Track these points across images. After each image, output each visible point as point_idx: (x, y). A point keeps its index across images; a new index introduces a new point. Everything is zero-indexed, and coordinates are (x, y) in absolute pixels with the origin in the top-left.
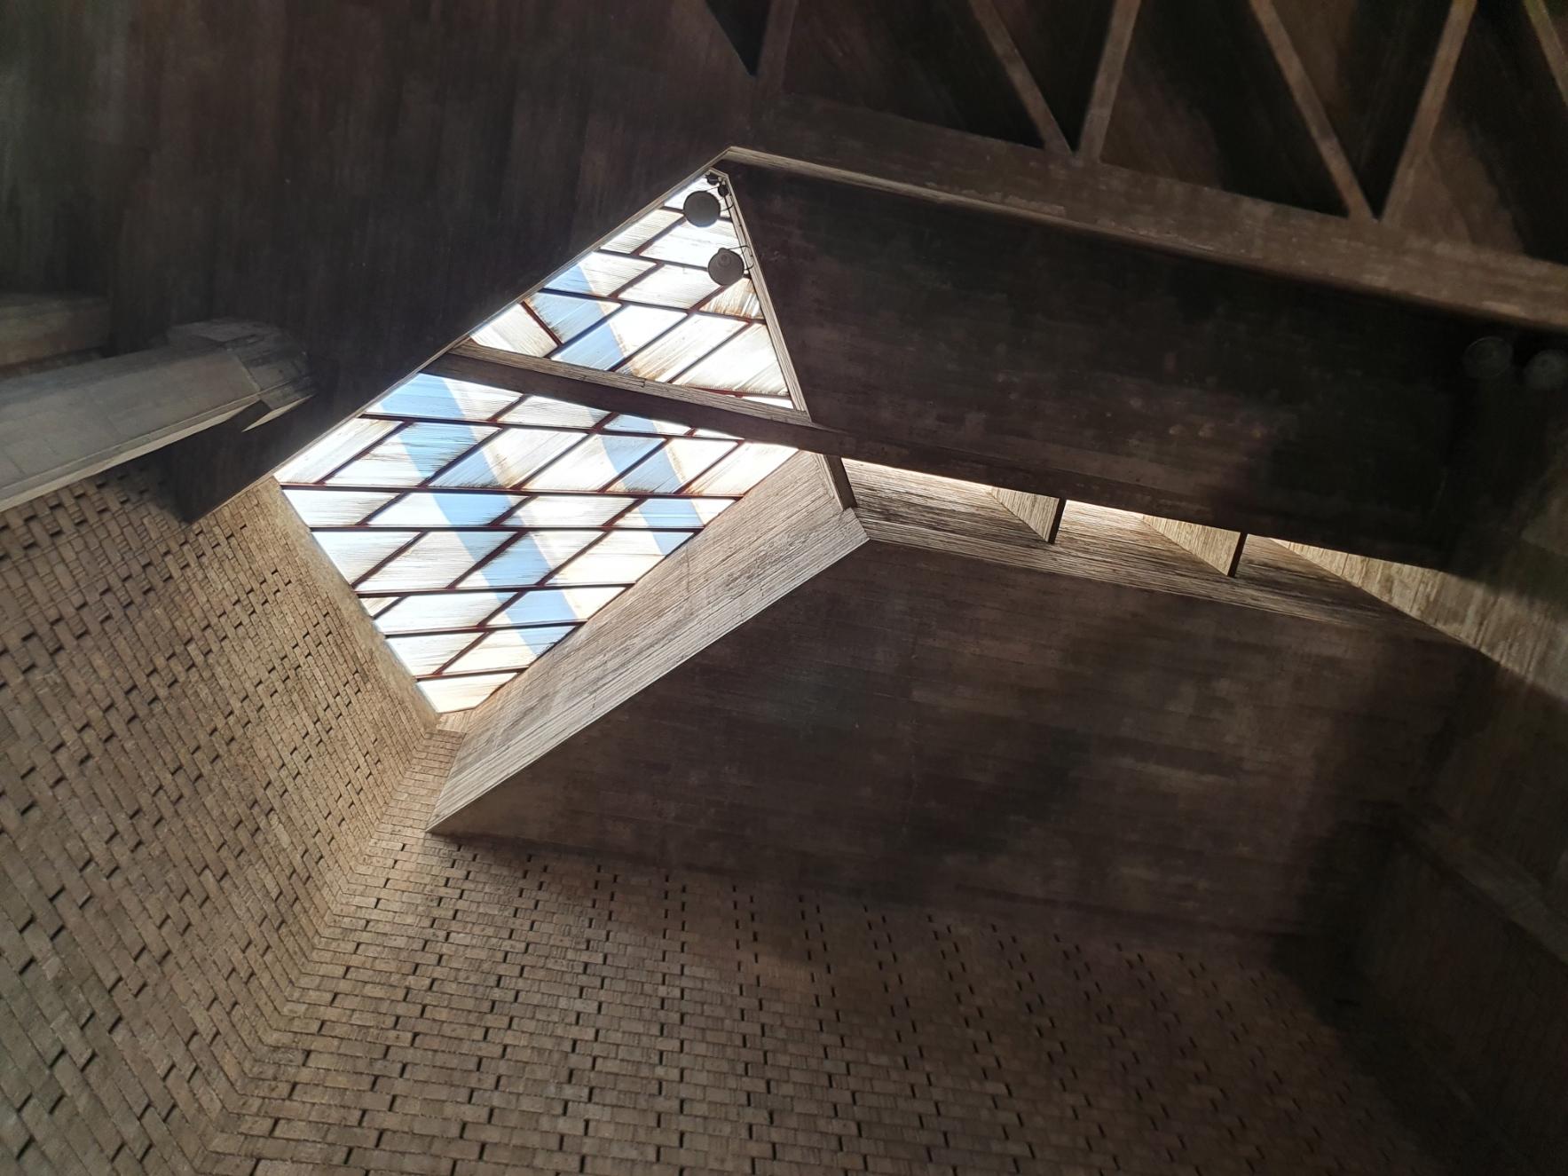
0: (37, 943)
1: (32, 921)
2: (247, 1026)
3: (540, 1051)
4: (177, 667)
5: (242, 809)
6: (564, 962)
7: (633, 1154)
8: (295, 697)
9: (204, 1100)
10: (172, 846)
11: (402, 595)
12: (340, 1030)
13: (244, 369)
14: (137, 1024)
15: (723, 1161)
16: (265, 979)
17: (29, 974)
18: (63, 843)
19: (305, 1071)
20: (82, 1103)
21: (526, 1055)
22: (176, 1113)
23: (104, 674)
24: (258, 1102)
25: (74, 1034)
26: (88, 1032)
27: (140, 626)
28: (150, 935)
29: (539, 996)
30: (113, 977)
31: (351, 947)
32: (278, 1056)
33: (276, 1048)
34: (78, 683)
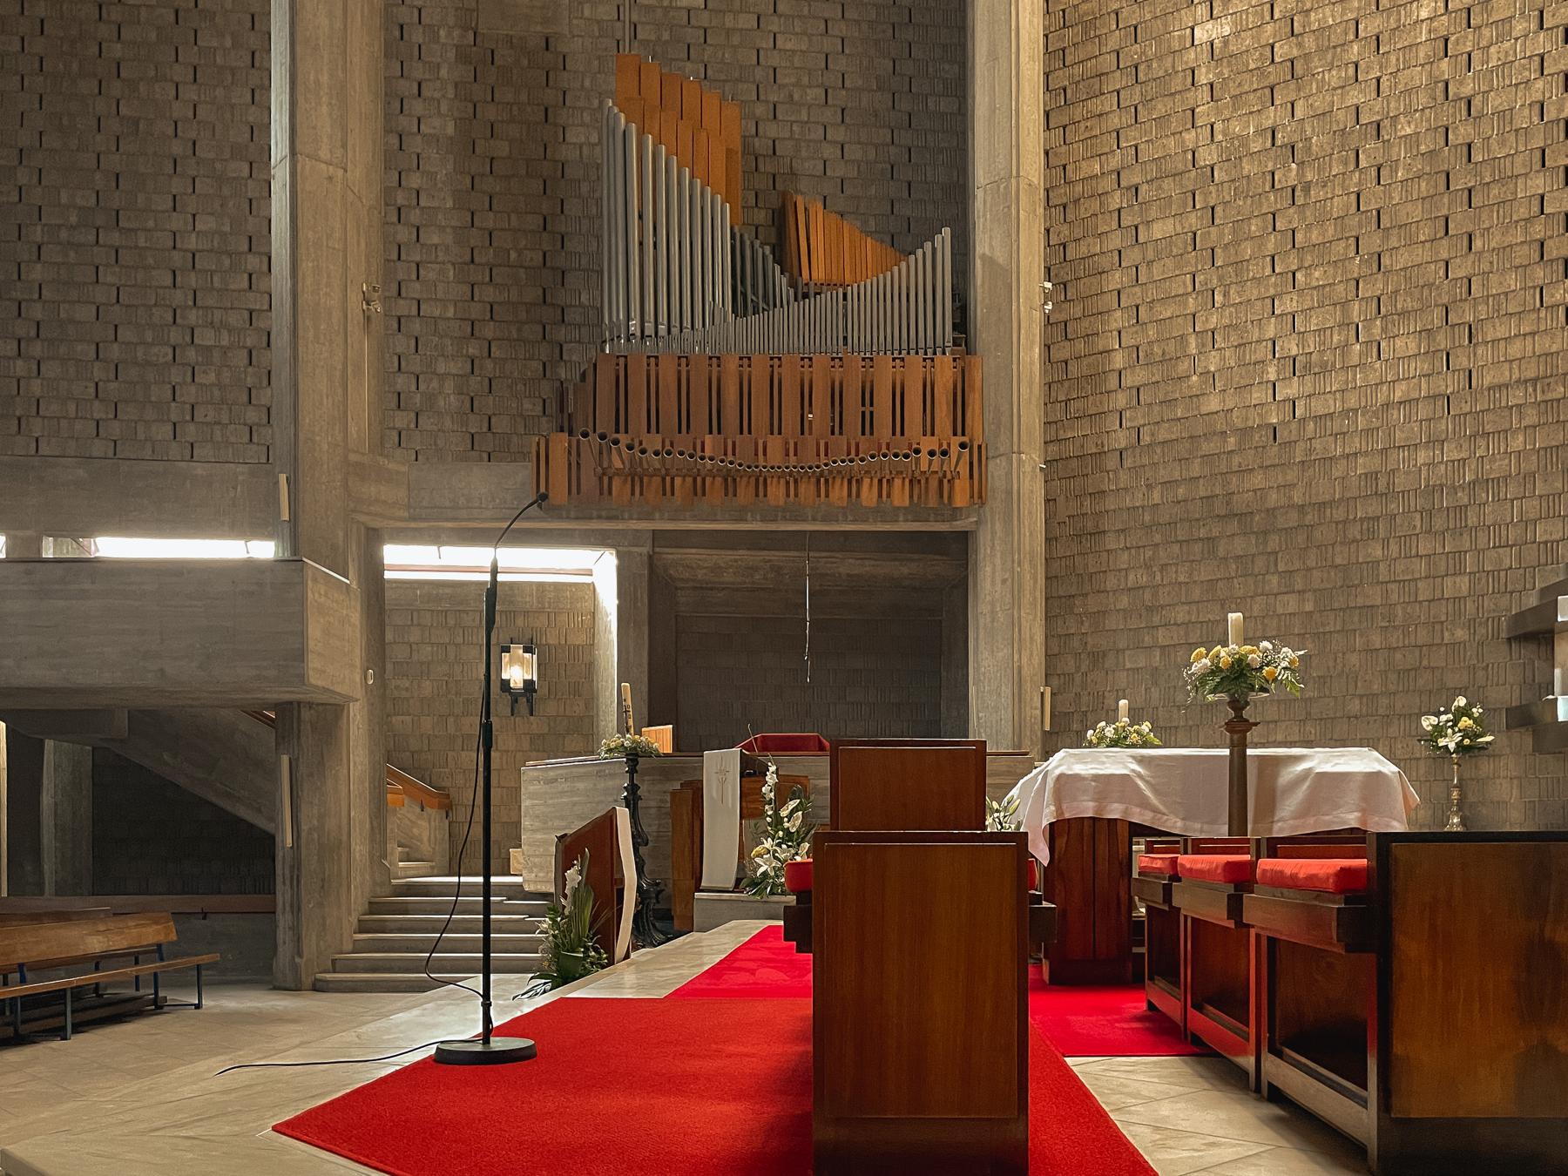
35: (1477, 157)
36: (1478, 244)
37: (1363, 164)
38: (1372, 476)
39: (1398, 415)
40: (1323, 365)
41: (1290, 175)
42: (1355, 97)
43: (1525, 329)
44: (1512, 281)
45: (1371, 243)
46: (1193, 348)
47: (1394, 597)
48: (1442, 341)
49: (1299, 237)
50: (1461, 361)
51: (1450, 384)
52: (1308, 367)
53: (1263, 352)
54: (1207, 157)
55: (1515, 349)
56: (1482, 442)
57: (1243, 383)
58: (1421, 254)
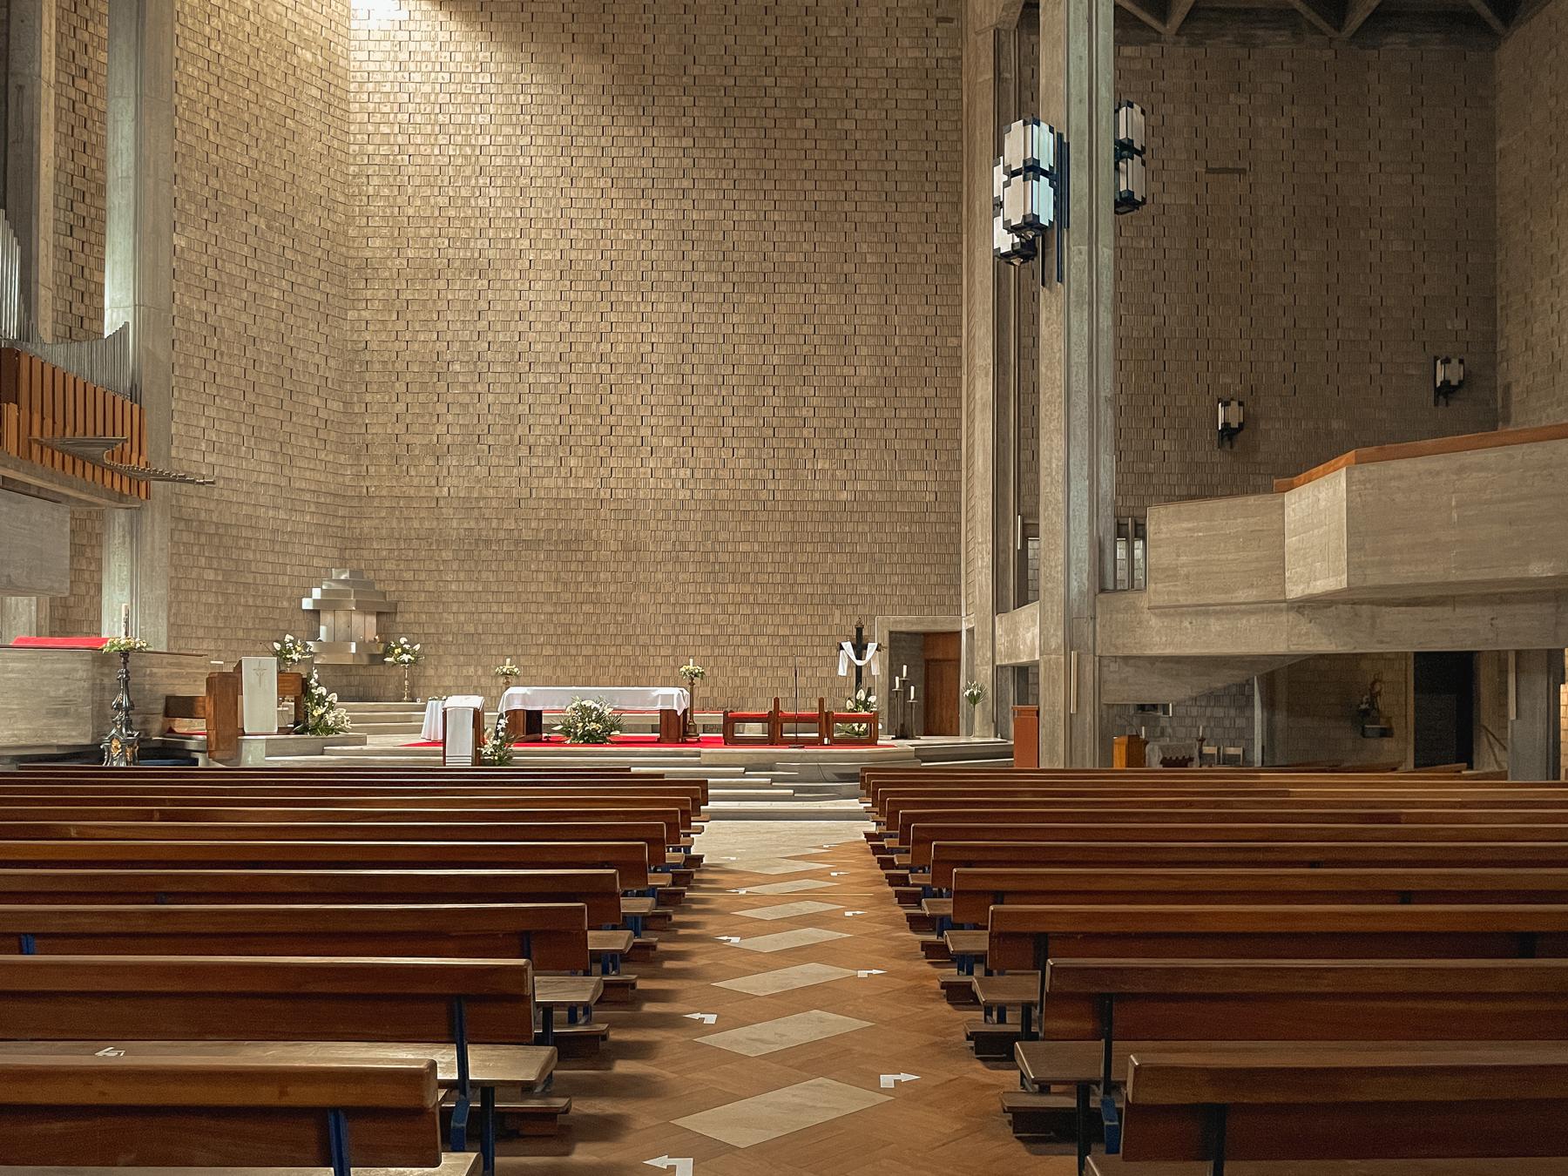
0: (253, 219)
3: (465, 156)
7: (510, 214)
10: (269, 125)
12: (377, 160)
15: (548, 212)
16: (336, 144)
19: (371, 188)
21: (459, 161)
30: (282, 206)
31: (365, 97)
33: (354, 176)
34: (191, 92)
35: (295, 377)
36: (294, 419)
37: (248, 355)
40: (228, 451)
43: (311, 466)
45: (251, 397)
47: (258, 582)
49: (218, 379)
50: (287, 471)
52: (220, 449)
53: (198, 433)
56: (294, 513)
57: (188, 446)
58: (272, 414)
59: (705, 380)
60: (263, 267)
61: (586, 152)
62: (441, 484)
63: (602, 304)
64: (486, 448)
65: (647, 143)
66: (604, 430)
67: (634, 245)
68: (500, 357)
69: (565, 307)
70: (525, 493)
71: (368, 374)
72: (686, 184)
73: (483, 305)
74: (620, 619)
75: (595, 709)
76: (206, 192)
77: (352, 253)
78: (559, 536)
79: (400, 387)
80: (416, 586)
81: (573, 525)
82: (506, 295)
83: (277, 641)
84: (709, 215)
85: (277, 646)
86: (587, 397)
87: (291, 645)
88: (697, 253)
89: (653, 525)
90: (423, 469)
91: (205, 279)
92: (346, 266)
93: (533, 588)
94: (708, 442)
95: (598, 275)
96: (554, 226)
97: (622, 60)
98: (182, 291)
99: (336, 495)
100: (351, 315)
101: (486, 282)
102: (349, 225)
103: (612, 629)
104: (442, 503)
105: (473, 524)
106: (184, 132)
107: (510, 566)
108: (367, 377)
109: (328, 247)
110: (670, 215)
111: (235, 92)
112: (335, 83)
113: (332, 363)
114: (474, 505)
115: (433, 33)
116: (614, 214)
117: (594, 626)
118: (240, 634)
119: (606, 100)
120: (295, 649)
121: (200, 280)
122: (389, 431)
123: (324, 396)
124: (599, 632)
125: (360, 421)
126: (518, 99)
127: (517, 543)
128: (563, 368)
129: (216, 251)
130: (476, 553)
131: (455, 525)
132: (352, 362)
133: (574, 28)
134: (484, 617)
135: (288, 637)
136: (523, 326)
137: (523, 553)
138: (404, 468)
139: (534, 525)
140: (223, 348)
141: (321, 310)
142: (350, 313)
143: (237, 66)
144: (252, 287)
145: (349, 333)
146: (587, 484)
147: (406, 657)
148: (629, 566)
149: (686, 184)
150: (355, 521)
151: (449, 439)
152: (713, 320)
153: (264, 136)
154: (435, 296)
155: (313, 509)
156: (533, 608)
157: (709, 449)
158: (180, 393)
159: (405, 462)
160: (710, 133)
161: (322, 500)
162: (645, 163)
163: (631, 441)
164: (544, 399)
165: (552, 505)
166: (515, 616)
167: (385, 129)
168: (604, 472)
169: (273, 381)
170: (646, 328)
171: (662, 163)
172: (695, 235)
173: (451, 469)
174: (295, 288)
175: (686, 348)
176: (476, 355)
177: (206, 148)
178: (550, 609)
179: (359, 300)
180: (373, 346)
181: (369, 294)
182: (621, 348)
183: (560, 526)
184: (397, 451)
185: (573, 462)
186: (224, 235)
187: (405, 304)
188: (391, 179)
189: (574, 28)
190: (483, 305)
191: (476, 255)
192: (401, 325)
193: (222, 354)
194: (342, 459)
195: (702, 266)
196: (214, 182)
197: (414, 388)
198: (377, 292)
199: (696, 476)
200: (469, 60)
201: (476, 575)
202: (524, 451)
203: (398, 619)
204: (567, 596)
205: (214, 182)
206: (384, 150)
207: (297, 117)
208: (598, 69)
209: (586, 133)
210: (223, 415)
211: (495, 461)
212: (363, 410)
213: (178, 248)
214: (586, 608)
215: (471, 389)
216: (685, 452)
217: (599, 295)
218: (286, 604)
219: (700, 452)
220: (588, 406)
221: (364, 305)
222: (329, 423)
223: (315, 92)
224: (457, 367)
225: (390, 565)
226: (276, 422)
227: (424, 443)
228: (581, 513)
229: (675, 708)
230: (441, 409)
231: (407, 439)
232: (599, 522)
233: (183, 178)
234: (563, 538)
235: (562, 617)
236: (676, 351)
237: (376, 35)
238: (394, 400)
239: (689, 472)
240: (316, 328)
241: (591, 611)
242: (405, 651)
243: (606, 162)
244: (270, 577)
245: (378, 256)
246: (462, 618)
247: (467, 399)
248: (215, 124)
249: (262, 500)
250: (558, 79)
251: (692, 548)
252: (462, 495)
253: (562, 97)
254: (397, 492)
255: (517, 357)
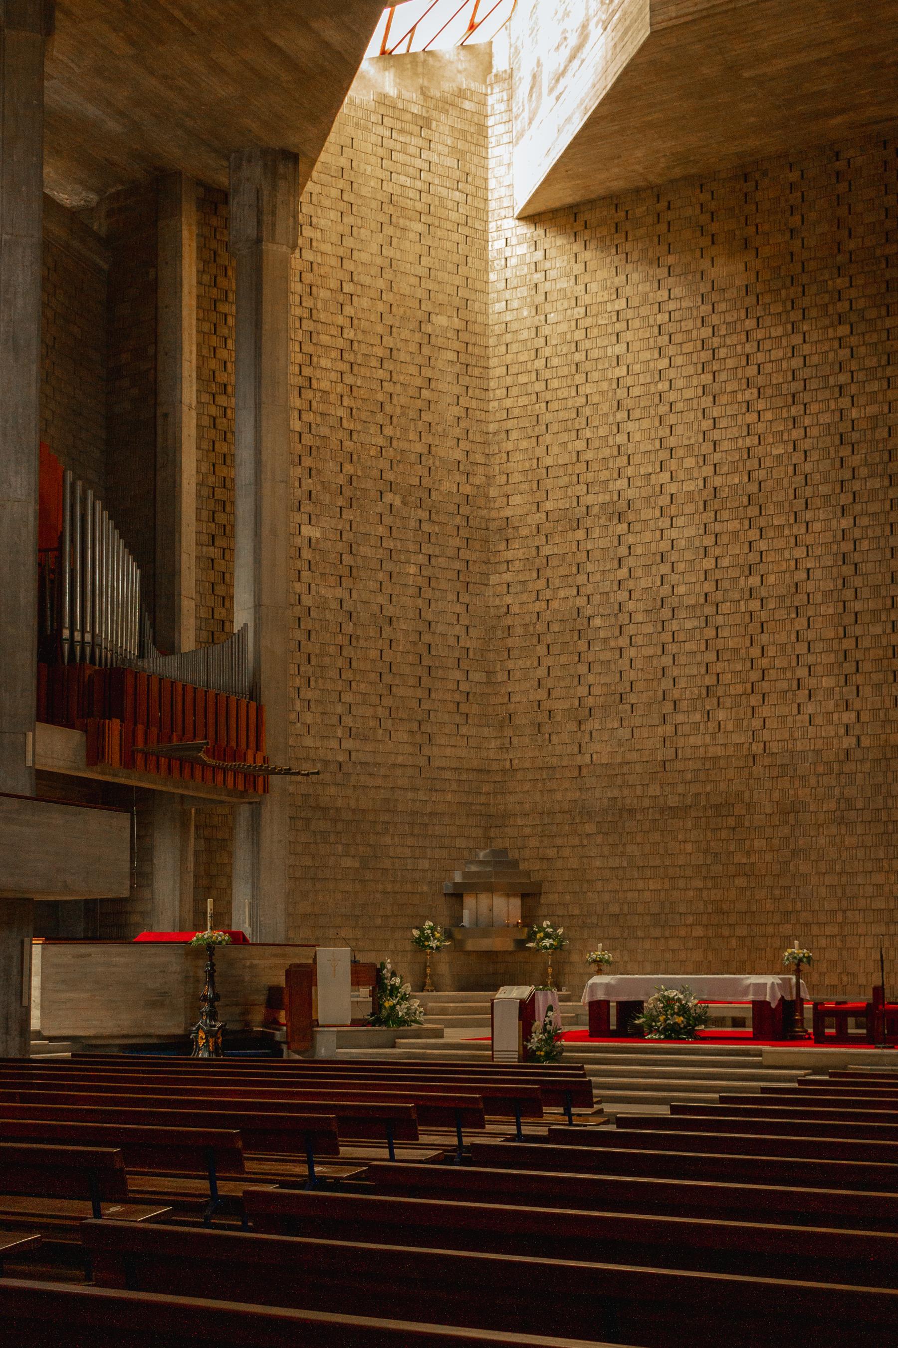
0: (389, 497)
1: (381, 493)
2: (478, 434)
3: (602, 393)
4: (348, 310)
5: (417, 337)
6: (606, 315)
7: (650, 447)
8: (401, 221)
9: (478, 483)
11: (412, 30)
12: (516, 412)
13: (275, 247)
14: (436, 486)
15: (689, 438)
16: (474, 404)
17: (394, 510)
18: (369, 455)
20: (437, 529)
22: (470, 498)
23: (329, 366)
24: (497, 468)
25: (419, 511)
26: (423, 506)
27: (323, 317)
28: (419, 448)
29: (597, 351)
30: (418, 479)
31: (503, 349)
32: (497, 438)
34: (325, 385)
35: (433, 653)
36: (433, 695)
37: (384, 636)
38: (387, 800)
39: (399, 772)
41: (349, 628)
42: (380, 599)
44: (446, 717)
45: (388, 679)
46: (298, 707)
47: (397, 866)
48: (418, 738)
50: (426, 751)
51: (422, 762)
52: (357, 734)
53: (335, 720)
54: (307, 601)
55: (448, 751)
56: (434, 794)
57: (325, 734)
59: (872, 605)
60: (399, 545)
61: (730, 363)
62: (583, 750)
63: (750, 533)
64: (628, 707)
65: (797, 339)
66: (755, 676)
67: (785, 459)
68: (641, 606)
69: (709, 541)
70: (670, 754)
71: (510, 640)
72: (843, 378)
73: (623, 551)
74: (777, 892)
75: (679, 1000)
76: (341, 479)
77: (493, 514)
78: (708, 799)
79: (541, 650)
80: (559, 864)
81: (723, 786)
82: (647, 536)
83: (417, 928)
84: (872, 410)
85: (416, 933)
86: (736, 640)
87: (429, 931)
88: (858, 457)
89: (813, 781)
90: (565, 737)
91: (341, 566)
92: (487, 529)
93: (681, 860)
94: (876, 678)
95: (745, 500)
96: (696, 453)
97: (766, 251)
98: (318, 581)
99: (479, 771)
100: (494, 579)
101: (625, 526)
102: (489, 485)
103: (769, 906)
104: (584, 772)
105: (616, 793)
106: (318, 425)
107: (656, 837)
108: (510, 642)
109: (467, 513)
110: (825, 418)
111: (368, 375)
112: (473, 341)
113: (474, 633)
114: (617, 772)
115: (568, 268)
116: (761, 428)
117: (749, 902)
118: (379, 921)
119: (751, 300)
120: (433, 935)
121: (336, 567)
122: (531, 698)
123: (466, 668)
124: (754, 908)
125: (503, 691)
126: (655, 320)
127: (662, 811)
128: (709, 610)
129: (351, 535)
130: (620, 824)
131: (598, 795)
132: (494, 628)
133: (714, 227)
134: (629, 895)
135: (429, 923)
136: (665, 569)
137: (669, 821)
138: (547, 736)
139: (680, 789)
140: (359, 633)
141: (461, 578)
142: (492, 577)
143: (370, 348)
144: (388, 566)
145: (491, 599)
146: (738, 738)
147: (547, 942)
148: (786, 831)
149: (843, 378)
150: (499, 797)
151: (590, 701)
152: (878, 532)
153: (398, 411)
154: (574, 549)
155: (454, 786)
156: (681, 883)
157: (878, 686)
158: (316, 682)
159: (546, 729)
160: (871, 314)
161: (464, 777)
162: (797, 363)
163: (784, 685)
164: (690, 646)
165: (699, 765)
166: (662, 894)
167: (523, 379)
168: (756, 723)
169: (411, 658)
170: (800, 552)
171: (815, 359)
172: (855, 436)
173: (594, 734)
174: (433, 560)
175: (848, 570)
176: (616, 606)
177: (340, 436)
178: (698, 883)
179: (500, 563)
180: (515, 609)
181: (509, 555)
182: (771, 579)
183: (708, 789)
184: (539, 720)
185: (721, 715)
186: (358, 519)
187: (545, 561)
188: (529, 430)
189: (714, 227)
190: (623, 551)
191: (615, 498)
192: (541, 584)
193: (358, 638)
194: (486, 731)
195: (863, 472)
196: (348, 468)
197: (555, 650)
198: (517, 552)
199: (862, 719)
200: (605, 288)
201: (620, 848)
202: (668, 707)
203: (543, 901)
204: (717, 869)
205: (348, 468)
206: (523, 401)
207: (433, 385)
208: (741, 267)
209: (728, 342)
210: (359, 699)
211: (637, 721)
212: (506, 678)
213: (313, 540)
214: (740, 882)
215: (612, 644)
216: (849, 692)
217: (746, 522)
218: (425, 888)
219: (867, 691)
220: (736, 650)
221: (505, 567)
222: (471, 696)
223: (452, 356)
224: (597, 622)
225: (534, 842)
226: (414, 700)
227: (566, 707)
228: (731, 773)
229: (768, 999)
230: (582, 669)
231: (547, 705)
232: (752, 781)
233: (317, 470)
234: (712, 802)
235: (713, 892)
236: (835, 575)
237: (513, 283)
238: (536, 664)
239: (853, 715)
240: (455, 599)
241: (745, 885)
242: (547, 936)
243: (752, 371)
244: (409, 861)
245: (518, 513)
246: (606, 897)
247: (607, 656)
248: (349, 410)
249: (400, 783)
250: (698, 289)
251: (860, 804)
252: (604, 761)
253: (703, 307)
254: (539, 763)
255: (659, 603)
